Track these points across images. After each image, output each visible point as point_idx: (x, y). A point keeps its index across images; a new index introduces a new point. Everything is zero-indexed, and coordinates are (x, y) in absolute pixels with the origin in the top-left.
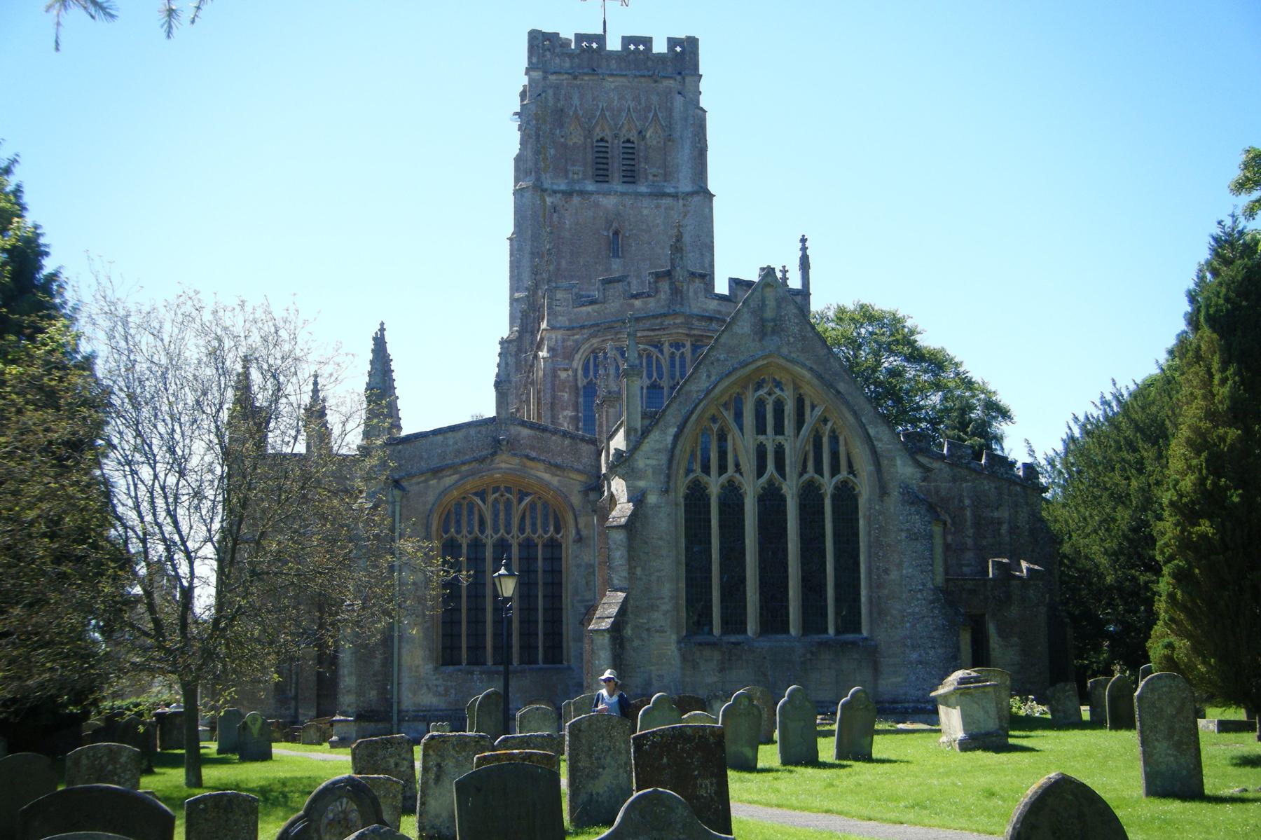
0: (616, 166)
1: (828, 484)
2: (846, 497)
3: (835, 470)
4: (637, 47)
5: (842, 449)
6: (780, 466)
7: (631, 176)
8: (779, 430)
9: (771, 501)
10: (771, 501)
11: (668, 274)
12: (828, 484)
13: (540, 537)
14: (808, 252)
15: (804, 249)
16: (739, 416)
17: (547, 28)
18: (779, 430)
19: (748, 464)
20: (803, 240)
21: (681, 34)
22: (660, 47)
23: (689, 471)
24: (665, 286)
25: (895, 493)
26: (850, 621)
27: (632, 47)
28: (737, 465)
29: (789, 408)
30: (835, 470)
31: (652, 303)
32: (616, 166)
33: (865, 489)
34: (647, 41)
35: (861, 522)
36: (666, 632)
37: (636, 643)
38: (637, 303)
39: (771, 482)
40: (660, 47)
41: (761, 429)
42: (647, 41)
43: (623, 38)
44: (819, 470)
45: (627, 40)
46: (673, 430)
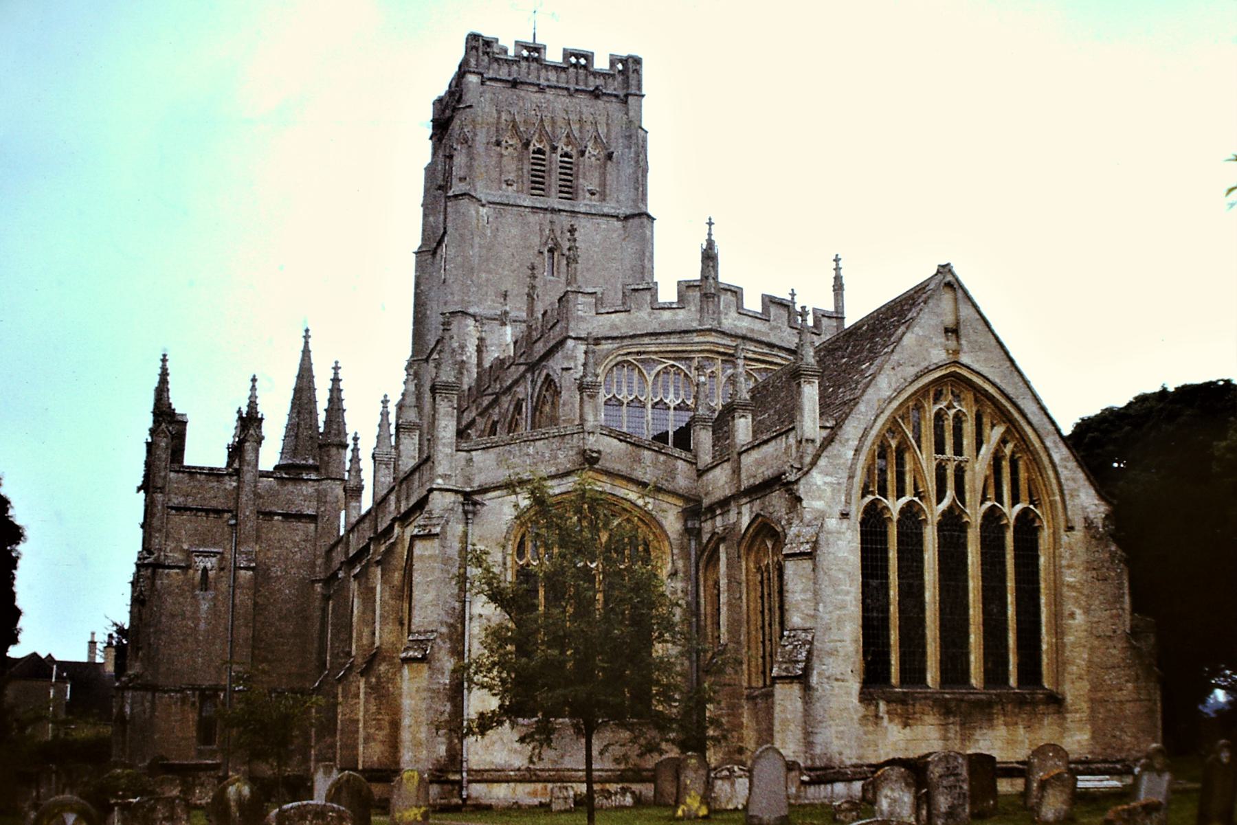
0: (554, 180)
4: (578, 61)
5: (1023, 475)
8: (958, 450)
14: (842, 273)
15: (837, 269)
17: (487, 33)
18: (958, 450)
20: (837, 260)
21: (623, 53)
22: (601, 63)
23: (865, 492)
26: (1030, 670)
27: (573, 60)
29: (969, 428)
31: (681, 314)
32: (554, 180)
34: (588, 57)
35: (1042, 560)
36: (847, 681)
40: (601, 63)
41: (940, 449)
42: (588, 57)
43: (565, 50)
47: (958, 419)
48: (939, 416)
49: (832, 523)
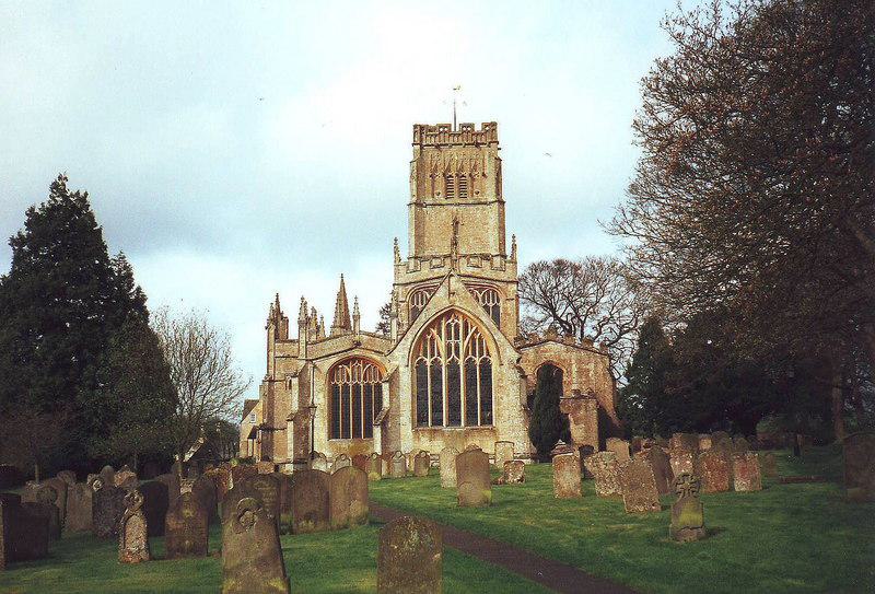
1: (478, 360)
2: (486, 368)
3: (481, 355)
6: (457, 354)
7: (462, 192)
8: (457, 337)
9: (453, 366)
10: (453, 366)
11: (450, 256)
12: (478, 360)
13: (372, 382)
16: (439, 333)
17: (422, 123)
19: (443, 352)
22: (478, 128)
24: (448, 261)
25: (506, 363)
26: (488, 420)
28: (439, 353)
30: (481, 355)
33: (494, 360)
37: (394, 429)
38: (436, 270)
39: (453, 359)
40: (478, 128)
41: (449, 337)
44: (474, 354)
45: (463, 126)
46: (411, 340)
47: (457, 326)
48: (449, 326)
49: (401, 369)
